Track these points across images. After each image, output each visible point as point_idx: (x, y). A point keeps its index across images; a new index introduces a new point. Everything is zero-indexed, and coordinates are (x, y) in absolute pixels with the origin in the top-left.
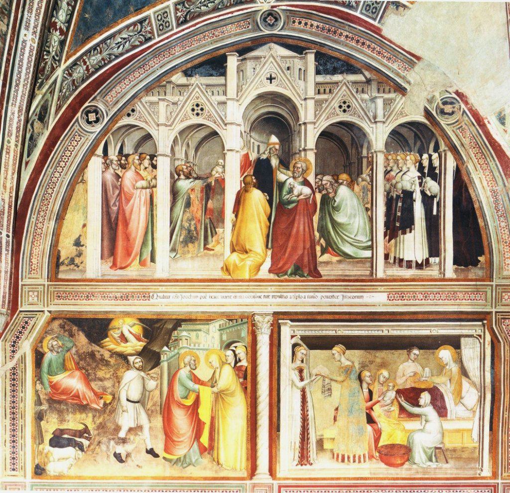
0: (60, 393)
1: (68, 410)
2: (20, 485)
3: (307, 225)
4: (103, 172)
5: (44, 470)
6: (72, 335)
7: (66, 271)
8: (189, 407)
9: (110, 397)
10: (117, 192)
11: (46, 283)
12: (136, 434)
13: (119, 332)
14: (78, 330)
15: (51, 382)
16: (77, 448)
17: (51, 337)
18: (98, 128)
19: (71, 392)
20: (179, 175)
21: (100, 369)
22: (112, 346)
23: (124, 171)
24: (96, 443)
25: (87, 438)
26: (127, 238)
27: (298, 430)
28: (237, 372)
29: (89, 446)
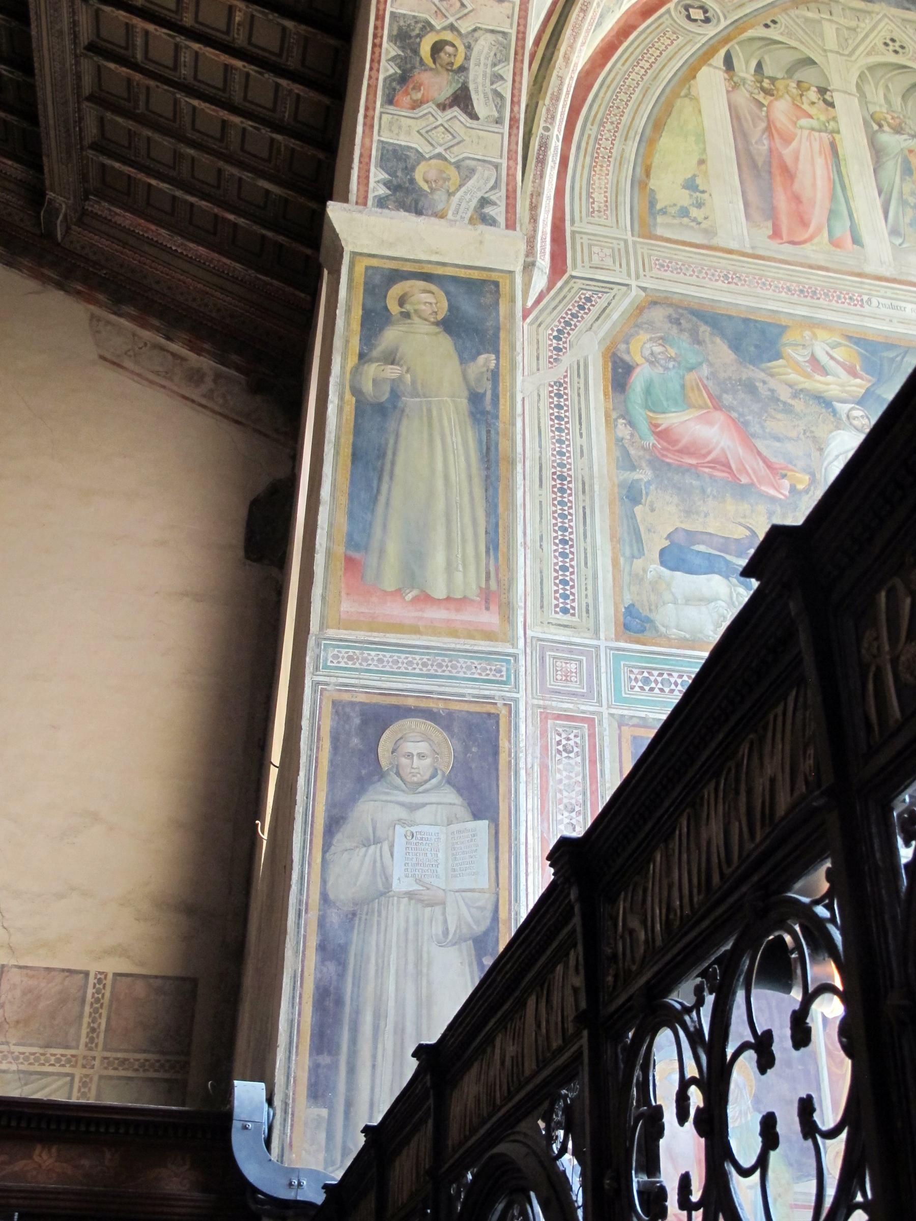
0: (681, 451)
1: (703, 491)
2: (581, 653)
4: (728, 92)
6: (697, 340)
7: (668, 225)
10: (763, 125)
11: (630, 239)
13: (806, 352)
14: (712, 334)
15: (657, 426)
17: (648, 336)
18: (711, 31)
19: (709, 453)
20: (880, 126)
22: (793, 377)
23: (770, 98)
26: (797, 199)
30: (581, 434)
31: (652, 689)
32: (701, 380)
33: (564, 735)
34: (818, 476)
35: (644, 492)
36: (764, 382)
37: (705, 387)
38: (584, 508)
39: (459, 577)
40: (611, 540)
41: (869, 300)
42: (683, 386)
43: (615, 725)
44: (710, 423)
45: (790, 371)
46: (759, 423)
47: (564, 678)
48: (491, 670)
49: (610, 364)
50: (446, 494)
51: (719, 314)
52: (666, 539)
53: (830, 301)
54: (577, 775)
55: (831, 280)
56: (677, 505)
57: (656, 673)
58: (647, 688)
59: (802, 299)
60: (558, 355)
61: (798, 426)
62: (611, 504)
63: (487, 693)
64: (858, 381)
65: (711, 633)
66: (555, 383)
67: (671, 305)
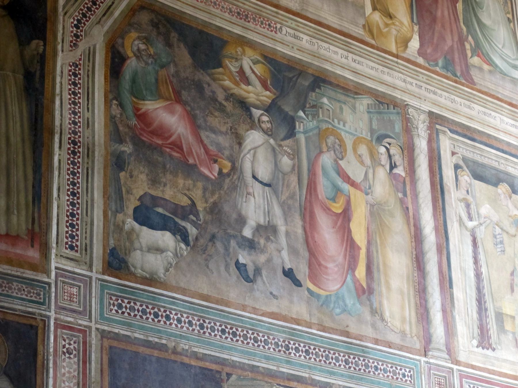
1: (164, 167)
2: (80, 281)
3: (451, 11)
5: (125, 262)
6: (169, 44)
8: (337, 215)
9: (228, 164)
12: (268, 239)
13: (237, 64)
14: (179, 40)
15: (138, 110)
16: (179, 237)
19: (170, 136)
21: (212, 114)
22: (227, 83)
24: (208, 236)
25: (194, 224)
27: (473, 294)
28: (394, 182)
29: (197, 239)
30: (88, 109)
31: (123, 313)
32: (169, 78)
33: (67, 341)
34: (237, 165)
35: (127, 161)
36: (209, 85)
37: (171, 82)
38: (87, 169)
39: (14, 219)
40: (104, 197)
41: (281, 28)
42: (157, 80)
43: (99, 336)
44: (172, 112)
45: (226, 78)
46: (203, 117)
47: (69, 299)
48: (33, 293)
49: (110, 54)
50: (7, 151)
51: (184, 24)
52: (139, 200)
53: (256, 25)
54: (74, 371)
55: (258, 8)
56: (147, 175)
57: (126, 301)
58: (120, 312)
59: (238, 20)
60: (76, 41)
61: (227, 123)
62: (105, 168)
63: (30, 310)
64: (268, 93)
65: (162, 275)
66: (73, 63)
67: (153, 11)
